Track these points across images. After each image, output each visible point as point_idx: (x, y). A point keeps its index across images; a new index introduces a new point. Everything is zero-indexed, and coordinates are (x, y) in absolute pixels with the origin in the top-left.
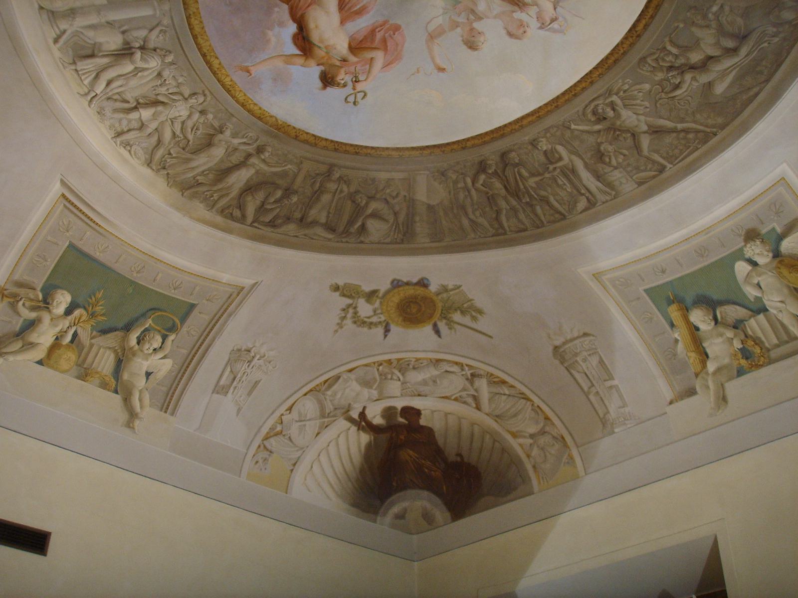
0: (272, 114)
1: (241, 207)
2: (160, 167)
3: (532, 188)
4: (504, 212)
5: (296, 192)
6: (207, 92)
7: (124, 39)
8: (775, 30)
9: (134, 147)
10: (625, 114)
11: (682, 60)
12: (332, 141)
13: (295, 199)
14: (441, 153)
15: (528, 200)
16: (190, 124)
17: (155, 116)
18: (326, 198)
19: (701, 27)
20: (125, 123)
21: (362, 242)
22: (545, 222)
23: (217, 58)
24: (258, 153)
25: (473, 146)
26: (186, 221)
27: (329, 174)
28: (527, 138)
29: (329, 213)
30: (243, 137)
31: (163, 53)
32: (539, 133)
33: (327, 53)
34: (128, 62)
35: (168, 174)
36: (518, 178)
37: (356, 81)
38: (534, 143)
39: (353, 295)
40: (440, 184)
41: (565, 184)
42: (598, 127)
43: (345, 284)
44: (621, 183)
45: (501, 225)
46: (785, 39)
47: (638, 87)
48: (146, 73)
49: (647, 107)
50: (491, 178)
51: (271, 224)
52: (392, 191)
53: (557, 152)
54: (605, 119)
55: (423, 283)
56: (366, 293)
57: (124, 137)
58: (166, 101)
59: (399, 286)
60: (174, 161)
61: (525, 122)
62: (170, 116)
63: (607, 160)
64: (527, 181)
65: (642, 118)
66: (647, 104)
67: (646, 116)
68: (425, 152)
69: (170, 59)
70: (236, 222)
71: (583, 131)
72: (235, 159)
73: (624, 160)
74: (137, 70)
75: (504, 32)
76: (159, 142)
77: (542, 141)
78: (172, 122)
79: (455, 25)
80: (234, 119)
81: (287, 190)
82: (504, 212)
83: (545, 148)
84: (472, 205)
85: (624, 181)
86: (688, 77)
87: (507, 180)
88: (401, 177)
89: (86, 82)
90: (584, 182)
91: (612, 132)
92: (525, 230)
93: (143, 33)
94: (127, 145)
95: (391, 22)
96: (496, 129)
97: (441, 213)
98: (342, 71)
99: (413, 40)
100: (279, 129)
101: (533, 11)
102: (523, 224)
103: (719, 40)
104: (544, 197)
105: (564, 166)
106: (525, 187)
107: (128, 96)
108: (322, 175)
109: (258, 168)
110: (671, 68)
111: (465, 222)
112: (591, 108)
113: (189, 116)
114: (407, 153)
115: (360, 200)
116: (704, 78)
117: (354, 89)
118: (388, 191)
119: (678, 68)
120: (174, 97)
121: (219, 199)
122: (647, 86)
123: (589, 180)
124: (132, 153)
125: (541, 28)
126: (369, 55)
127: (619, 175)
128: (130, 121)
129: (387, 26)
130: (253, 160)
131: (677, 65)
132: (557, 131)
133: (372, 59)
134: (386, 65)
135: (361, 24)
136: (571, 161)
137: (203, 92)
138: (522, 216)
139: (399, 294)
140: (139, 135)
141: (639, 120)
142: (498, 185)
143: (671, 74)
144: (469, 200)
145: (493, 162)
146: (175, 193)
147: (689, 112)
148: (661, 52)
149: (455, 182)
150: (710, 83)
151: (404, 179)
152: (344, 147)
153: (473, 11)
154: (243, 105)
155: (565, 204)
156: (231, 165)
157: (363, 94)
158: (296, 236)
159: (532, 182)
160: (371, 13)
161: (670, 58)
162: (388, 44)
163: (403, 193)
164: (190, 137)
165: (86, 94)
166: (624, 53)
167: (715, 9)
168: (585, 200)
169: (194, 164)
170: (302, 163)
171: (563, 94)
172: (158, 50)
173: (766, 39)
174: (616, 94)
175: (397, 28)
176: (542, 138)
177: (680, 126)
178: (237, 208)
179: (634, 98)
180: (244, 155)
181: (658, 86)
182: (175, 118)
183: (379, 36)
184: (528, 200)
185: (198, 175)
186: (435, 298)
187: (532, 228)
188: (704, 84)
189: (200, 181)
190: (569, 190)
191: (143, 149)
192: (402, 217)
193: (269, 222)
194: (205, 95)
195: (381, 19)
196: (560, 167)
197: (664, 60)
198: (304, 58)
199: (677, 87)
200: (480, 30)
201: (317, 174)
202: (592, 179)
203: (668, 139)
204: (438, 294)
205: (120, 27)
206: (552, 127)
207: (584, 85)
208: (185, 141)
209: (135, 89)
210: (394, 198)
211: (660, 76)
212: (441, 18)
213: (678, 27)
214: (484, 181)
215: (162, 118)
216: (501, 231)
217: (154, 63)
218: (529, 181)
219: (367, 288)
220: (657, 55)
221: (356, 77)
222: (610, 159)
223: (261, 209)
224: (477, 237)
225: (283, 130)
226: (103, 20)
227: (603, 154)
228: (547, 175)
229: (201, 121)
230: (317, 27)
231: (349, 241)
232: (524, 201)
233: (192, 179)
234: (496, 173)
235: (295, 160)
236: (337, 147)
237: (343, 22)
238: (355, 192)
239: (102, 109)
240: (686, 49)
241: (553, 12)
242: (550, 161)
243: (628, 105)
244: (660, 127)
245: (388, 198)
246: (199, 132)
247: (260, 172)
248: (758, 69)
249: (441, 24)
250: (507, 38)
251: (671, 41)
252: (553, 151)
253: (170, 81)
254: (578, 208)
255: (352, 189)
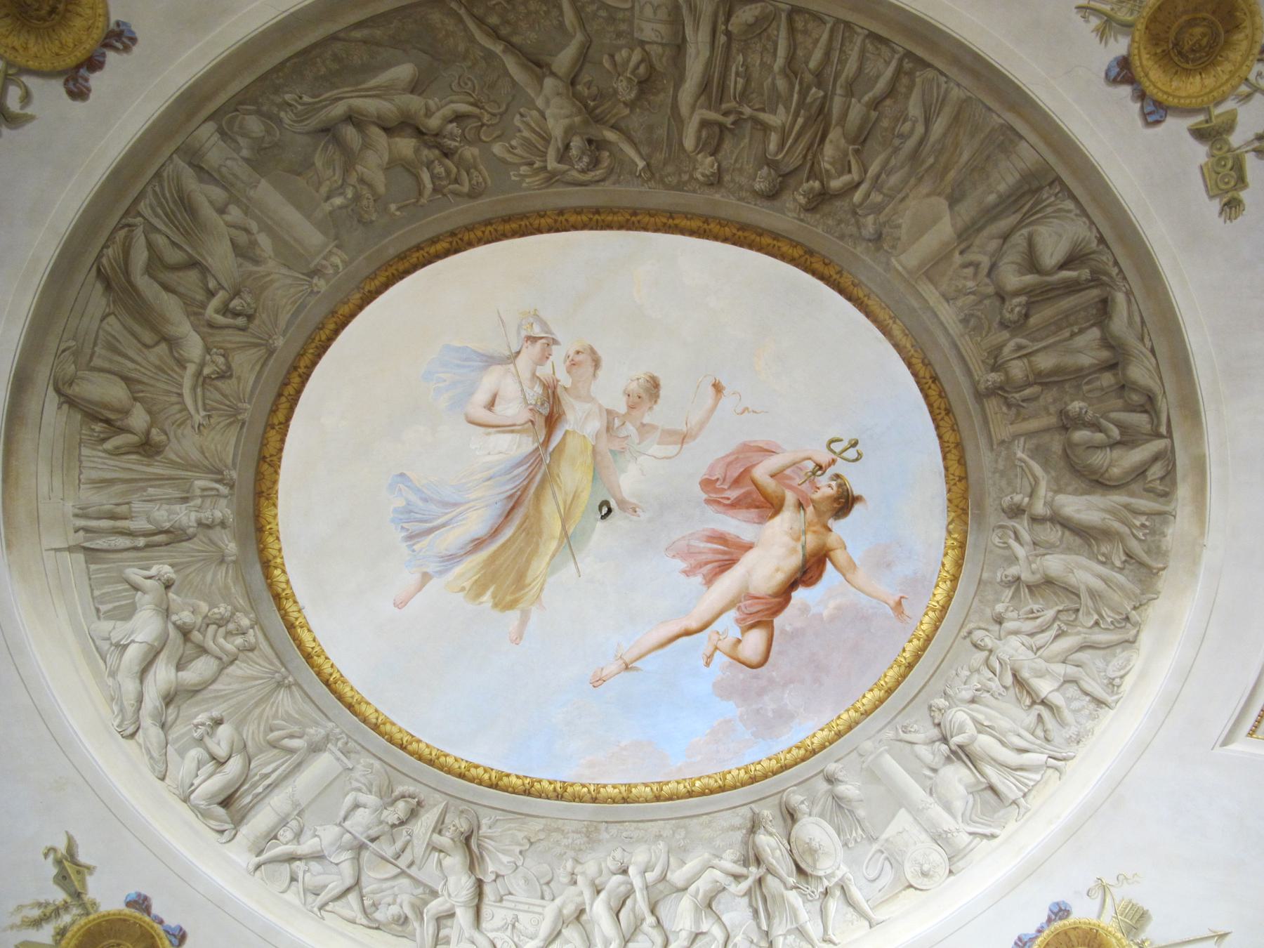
0: (944, 533)
1: (1140, 472)
2: (1129, 625)
3: (787, 109)
4: (866, 98)
5: (1063, 413)
6: (964, 632)
7: (944, 765)
8: (282, 114)
9: (1111, 674)
10: (556, 128)
11: (426, 153)
12: (937, 427)
13: (1076, 406)
14: (845, 274)
15: (814, 90)
16: (1029, 626)
17: (1040, 675)
18: (1045, 362)
19: (370, 186)
20: (1076, 705)
21: (1102, 240)
22: (829, 26)
23: (904, 650)
24: (1023, 511)
25: (795, 244)
26: (1214, 537)
27: (998, 391)
28: (717, 196)
29: (1073, 335)
30: (1009, 547)
31: (937, 714)
32: (694, 191)
33: (805, 533)
34: (976, 745)
35: (1135, 608)
36: (790, 141)
37: (821, 468)
38: (715, 181)
39: (1230, 165)
40: (899, 226)
41: (737, 74)
42: (610, 135)
43: (1211, 197)
44: (656, 9)
45: (899, 71)
46: (277, 90)
47: (509, 157)
48: (980, 717)
49: (522, 115)
50: (827, 171)
51: (1148, 407)
52: (965, 278)
53: (698, 138)
54: (590, 142)
55: (1123, 72)
56: (1211, 147)
57: (1099, 692)
58: (1009, 674)
59: (1158, 105)
60: (1106, 612)
61: (694, 224)
62: (1031, 655)
63: (642, 70)
64: (783, 127)
65: (540, 103)
66: (517, 121)
67: (533, 101)
68: (861, 295)
69: (941, 702)
70: (1174, 464)
71: (635, 145)
72: (1053, 534)
73: (619, 48)
74: (981, 728)
75: (600, 373)
76: (1082, 648)
77: (703, 175)
78: (1038, 649)
79: (644, 429)
80: (985, 575)
81: (1065, 428)
82: (866, 98)
83: (710, 159)
84: (896, 150)
85: (648, 11)
86: (434, 123)
87: (808, 149)
88: (932, 287)
89: (1037, 777)
90: (708, 54)
91: (598, 111)
92: (874, 37)
93: (923, 751)
94: (1113, 685)
95: (705, 496)
96: (741, 246)
97: (952, 174)
98: (817, 496)
99: (709, 452)
100: (965, 511)
101: (544, 371)
102: (863, 51)
103: (361, 150)
104: (787, 76)
105: (709, 108)
106: (797, 115)
107: (1030, 719)
108: (1006, 398)
109: (1050, 494)
110: (447, 154)
111: (938, 127)
112: (593, 174)
113: (1016, 633)
114: (882, 315)
115: (1017, 309)
116: (415, 103)
117: (834, 461)
118: (970, 284)
119: (438, 146)
120: (997, 666)
121: (1143, 513)
122: (497, 149)
123: (698, 53)
124: (1122, 672)
125: (555, 342)
126: (770, 485)
127: (645, 25)
128: (1069, 700)
129: (714, 496)
130: (1040, 508)
131: (437, 152)
132: (669, 175)
133: (772, 476)
134: (768, 452)
135: (736, 525)
136: (693, 108)
137: (965, 638)
138: (851, 67)
139: (1178, 89)
140: (1087, 678)
141: (547, 102)
142: (829, 151)
143: (454, 144)
144: (893, 162)
145: (796, 197)
146: (1163, 583)
147: (470, 64)
148: (444, 187)
149: (877, 209)
150: (412, 92)
151: (931, 280)
152: (936, 405)
153: (609, 429)
154: (955, 579)
155: (769, 38)
156: (1067, 533)
157: (833, 446)
158: (1153, 351)
159: (777, 119)
160: (712, 526)
161: (439, 170)
162: (736, 475)
163: (957, 259)
164: (1050, 613)
165: (1056, 769)
166: (488, 223)
167: (338, 201)
168: (733, 20)
169: (1097, 584)
170: (1003, 442)
171: (609, 226)
172: (937, 721)
173: (300, 107)
174: (544, 168)
175: (707, 484)
176: (697, 179)
177: (498, 48)
178: (1145, 477)
179: (528, 144)
180: (1037, 527)
181: (483, 138)
182: (1030, 648)
183: (734, 494)
184: (814, 90)
185: (1113, 567)
186: (1141, 26)
187: (859, 30)
188: (420, 95)
189: (1124, 558)
190: (740, 58)
191: (1107, 664)
192: (1004, 224)
193: (1146, 412)
194: (970, 633)
195: (710, 511)
196: (717, 110)
197: (448, 172)
198: (832, 553)
199: (458, 118)
200: (625, 398)
201: (1009, 406)
202: (691, 50)
203: (528, 37)
204: (1128, 26)
205: (931, 778)
206: (669, 187)
207: (573, 218)
208: (1063, 617)
209: (1012, 717)
210: (976, 265)
211: (470, 152)
212: (650, 452)
213: (398, 209)
214: (841, 174)
215: (1041, 664)
216: (907, 65)
217: (959, 715)
218: (779, 122)
219: (1200, 152)
220: (451, 187)
221: (814, 473)
222: (637, 67)
223: (1128, 439)
224: (952, 84)
225: (961, 505)
226: (930, 800)
227: (640, 83)
228: (747, 111)
229: (1015, 614)
230: (777, 570)
231: (1111, 263)
232: (821, 93)
233: (1126, 572)
234: (812, 175)
235: (1004, 453)
236: (943, 413)
237: (749, 547)
238: (1007, 327)
239: (1069, 741)
240: (410, 168)
241: (524, 350)
242: (721, 131)
243: (543, 138)
244: (524, 66)
245: (986, 271)
246: (1036, 607)
247: (1055, 488)
248: (335, 66)
249: (659, 444)
250: (604, 364)
251: (420, 194)
252: (701, 146)
253: (975, 682)
254: (757, 12)
255: (1006, 334)
